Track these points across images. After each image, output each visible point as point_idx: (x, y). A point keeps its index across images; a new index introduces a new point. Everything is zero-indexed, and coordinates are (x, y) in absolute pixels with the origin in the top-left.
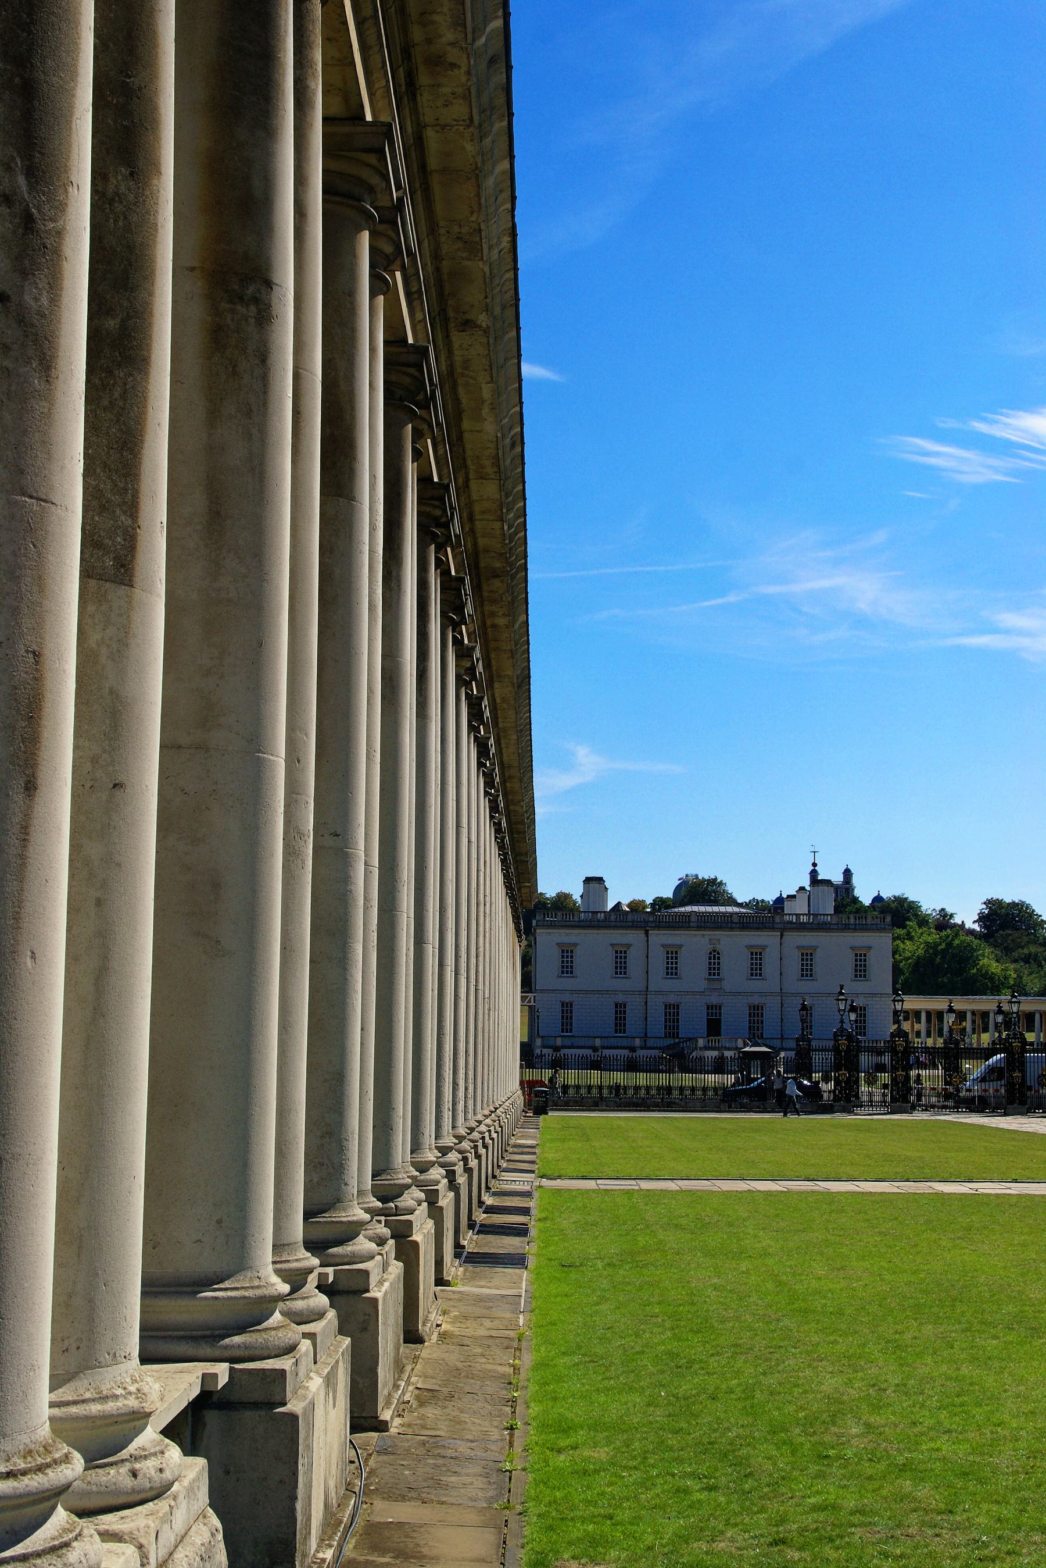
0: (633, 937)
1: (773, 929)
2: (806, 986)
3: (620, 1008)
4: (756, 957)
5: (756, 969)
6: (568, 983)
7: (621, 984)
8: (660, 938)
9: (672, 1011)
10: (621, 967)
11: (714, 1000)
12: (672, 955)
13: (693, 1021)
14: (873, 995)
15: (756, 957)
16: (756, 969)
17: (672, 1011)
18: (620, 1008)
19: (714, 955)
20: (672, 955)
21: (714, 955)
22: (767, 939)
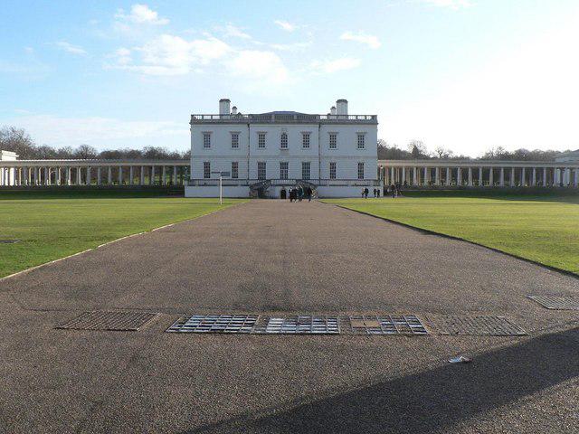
0: (242, 129)
1: (315, 123)
2: (332, 152)
3: (235, 166)
4: (306, 137)
5: (306, 144)
6: (207, 152)
7: (235, 152)
8: (256, 128)
9: (262, 166)
10: (235, 145)
11: (284, 160)
12: (262, 136)
13: (273, 172)
14: (367, 157)
15: (306, 137)
16: (306, 144)
17: (262, 166)
18: (235, 166)
19: (284, 138)
20: (262, 136)
21: (284, 138)
22: (313, 129)
